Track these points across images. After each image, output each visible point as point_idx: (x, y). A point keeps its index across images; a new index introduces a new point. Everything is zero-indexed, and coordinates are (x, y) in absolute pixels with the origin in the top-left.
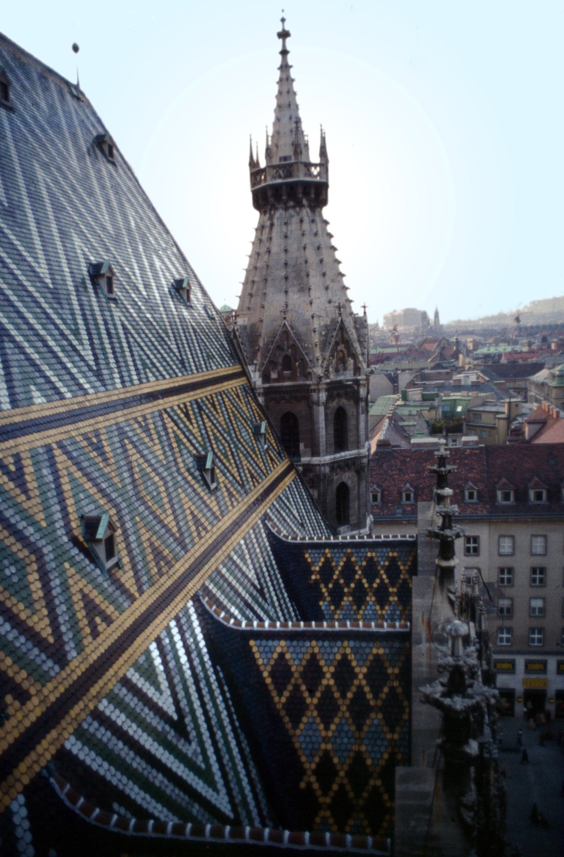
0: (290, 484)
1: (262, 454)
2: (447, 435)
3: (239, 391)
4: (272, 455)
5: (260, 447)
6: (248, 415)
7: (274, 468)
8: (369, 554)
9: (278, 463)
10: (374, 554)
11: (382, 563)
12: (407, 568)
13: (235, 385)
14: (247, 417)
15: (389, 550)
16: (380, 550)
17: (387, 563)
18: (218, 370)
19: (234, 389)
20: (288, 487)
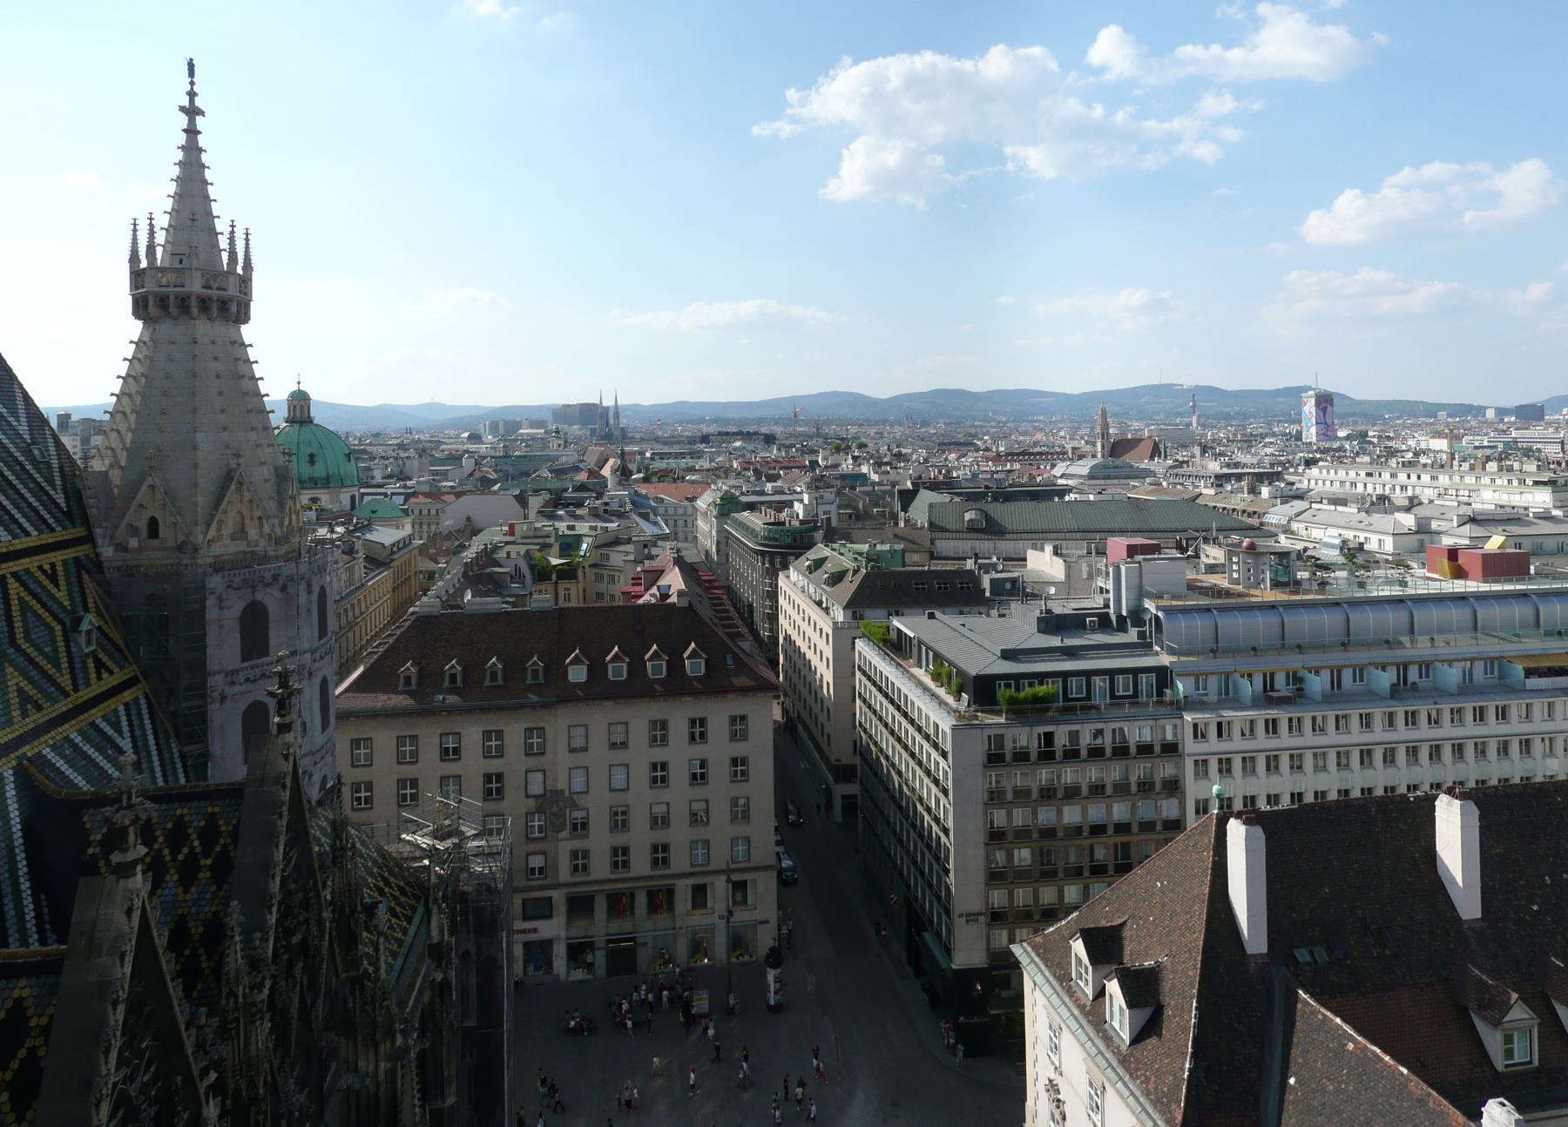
0: (136, 699)
1: (78, 660)
2: (556, 583)
3: (60, 568)
4: (105, 659)
5: (74, 650)
6: (66, 603)
7: (99, 678)
8: (179, 812)
9: (116, 670)
10: (185, 811)
11: (195, 824)
12: (230, 828)
13: (54, 560)
14: (64, 608)
15: (208, 803)
16: (195, 804)
17: (202, 823)
18: (17, 541)
19: (47, 567)
20: (126, 705)
